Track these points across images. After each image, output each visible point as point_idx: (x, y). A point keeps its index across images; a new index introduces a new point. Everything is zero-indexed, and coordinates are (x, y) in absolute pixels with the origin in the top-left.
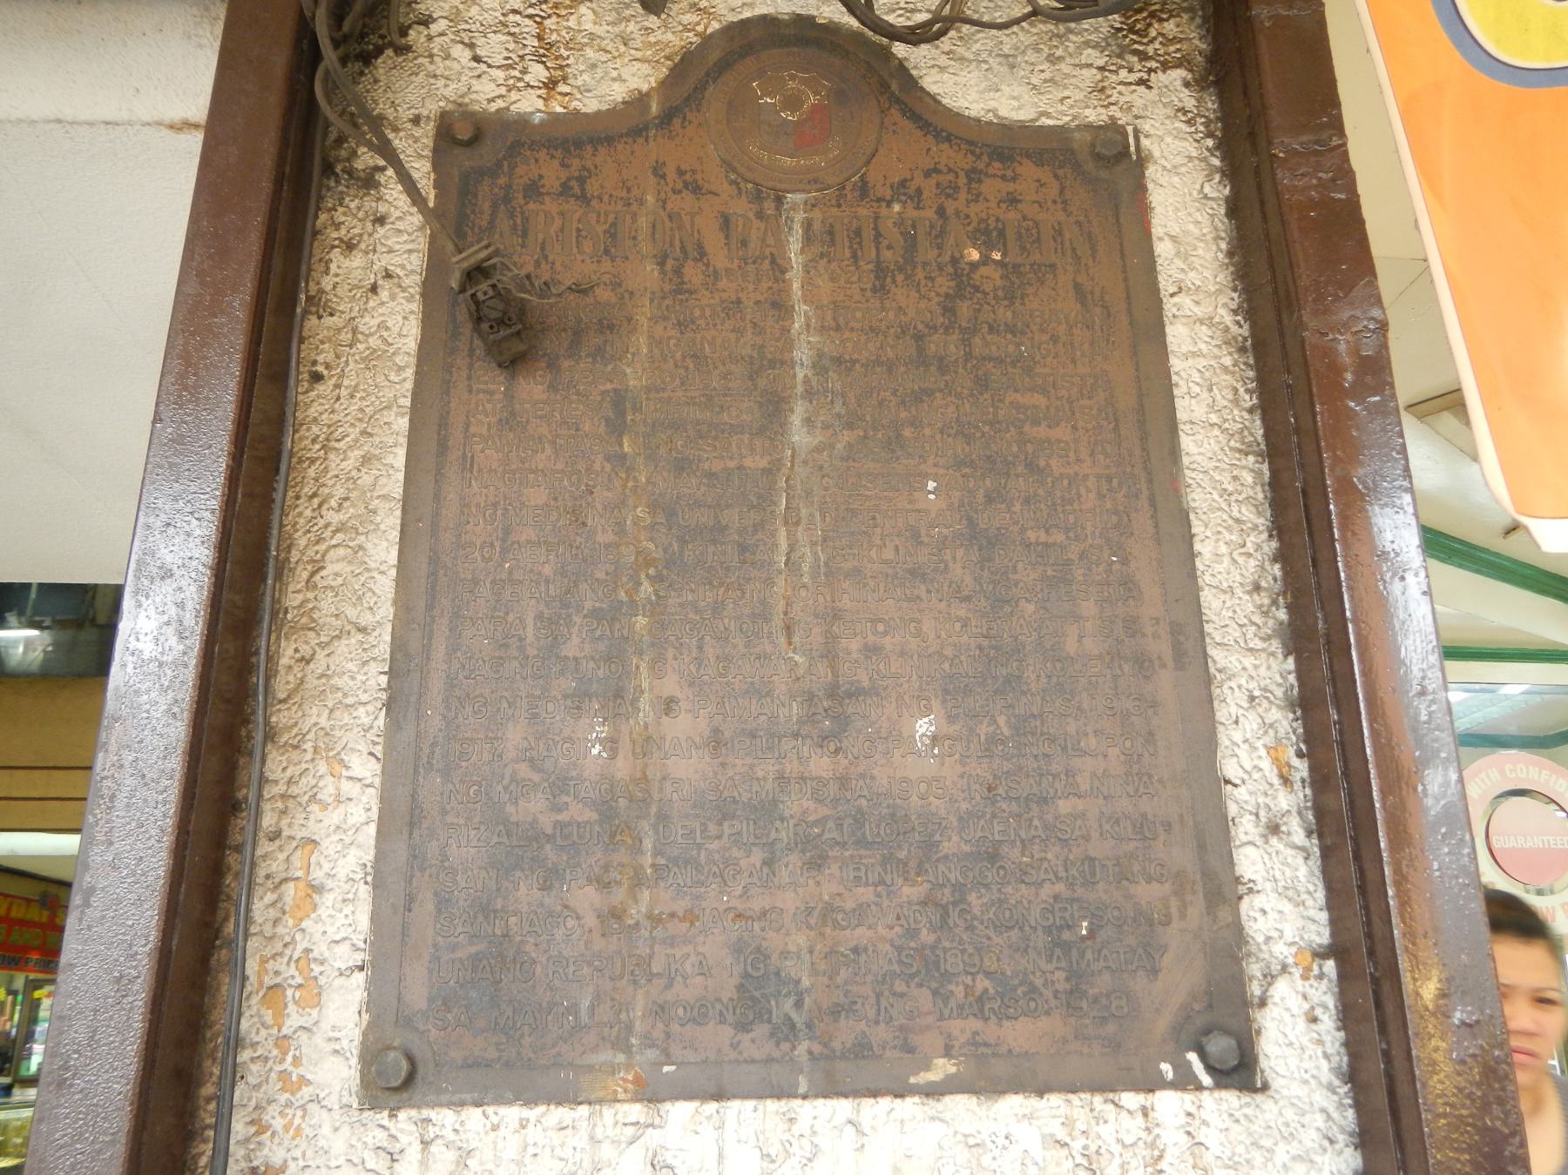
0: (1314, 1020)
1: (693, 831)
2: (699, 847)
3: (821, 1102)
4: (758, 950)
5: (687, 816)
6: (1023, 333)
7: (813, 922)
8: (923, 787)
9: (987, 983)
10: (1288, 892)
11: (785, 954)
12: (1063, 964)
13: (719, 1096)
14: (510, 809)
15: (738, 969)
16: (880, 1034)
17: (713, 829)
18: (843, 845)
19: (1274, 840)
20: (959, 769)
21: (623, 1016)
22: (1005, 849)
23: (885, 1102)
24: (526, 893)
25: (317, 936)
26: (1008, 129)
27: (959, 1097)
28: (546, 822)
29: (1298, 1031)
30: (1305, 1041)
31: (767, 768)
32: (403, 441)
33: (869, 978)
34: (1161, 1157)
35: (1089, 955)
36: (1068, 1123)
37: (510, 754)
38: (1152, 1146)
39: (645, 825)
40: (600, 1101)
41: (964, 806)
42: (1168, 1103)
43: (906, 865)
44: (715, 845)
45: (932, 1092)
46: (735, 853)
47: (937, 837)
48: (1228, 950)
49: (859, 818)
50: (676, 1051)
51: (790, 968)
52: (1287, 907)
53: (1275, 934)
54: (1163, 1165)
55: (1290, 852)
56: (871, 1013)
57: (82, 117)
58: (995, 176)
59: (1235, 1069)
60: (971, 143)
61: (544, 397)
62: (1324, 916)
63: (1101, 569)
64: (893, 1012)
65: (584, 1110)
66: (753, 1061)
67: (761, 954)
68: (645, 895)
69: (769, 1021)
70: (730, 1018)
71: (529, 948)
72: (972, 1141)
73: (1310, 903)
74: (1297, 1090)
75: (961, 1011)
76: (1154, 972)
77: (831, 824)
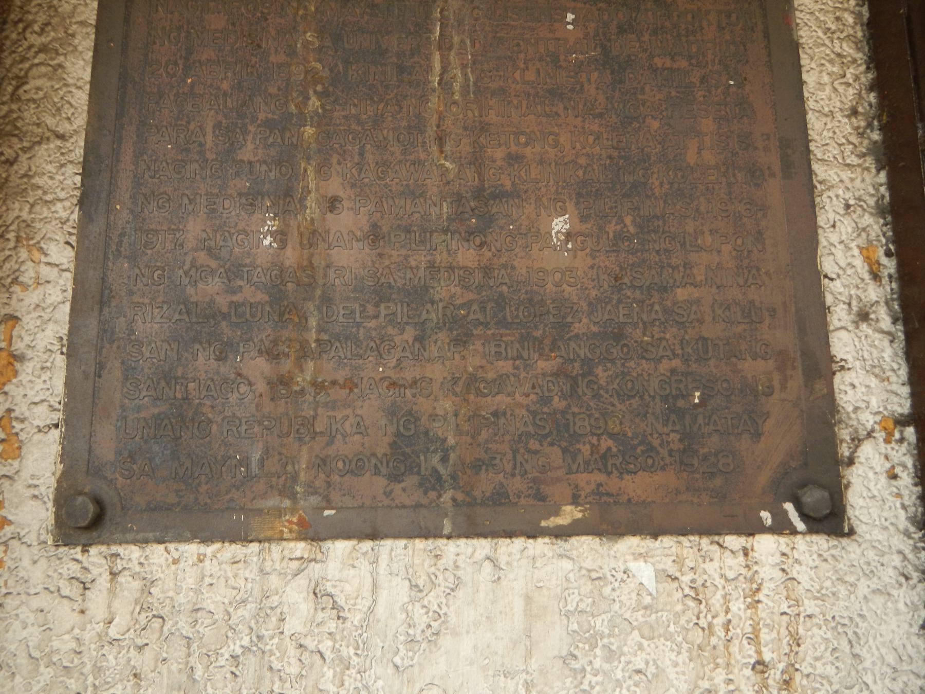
0: (895, 477)
1: (353, 312)
2: (359, 325)
3: (462, 542)
4: (410, 413)
5: (348, 299)
7: (458, 389)
8: (558, 276)
9: (610, 443)
10: (876, 371)
11: (433, 417)
13: (374, 535)
14: (190, 290)
15: (391, 429)
16: (517, 484)
17: (371, 310)
18: (486, 325)
19: (864, 326)
20: (589, 261)
21: (289, 468)
22: (629, 330)
23: (519, 543)
24: (204, 362)
25: (18, 399)
27: (584, 538)
28: (222, 302)
30: (886, 494)
31: (419, 259)
33: (507, 438)
34: (758, 590)
35: (700, 420)
36: (679, 561)
37: (190, 244)
38: (751, 580)
39: (311, 306)
40: (269, 540)
41: (594, 293)
43: (541, 342)
44: (372, 324)
45: (561, 533)
46: (390, 330)
47: (569, 319)
48: (823, 415)
49: (501, 302)
50: (336, 497)
51: (438, 428)
52: (873, 382)
53: (863, 405)
54: (760, 596)
55: (877, 335)
56: (509, 468)
59: (826, 517)
62: (906, 390)
63: (719, 91)
64: (528, 467)
65: (254, 547)
66: (404, 507)
67: (412, 417)
68: (310, 365)
69: (419, 473)
70: (384, 470)
71: (205, 410)
72: (594, 575)
73: (894, 379)
74: (877, 535)
75: (587, 467)
76: (757, 435)
77: (475, 307)
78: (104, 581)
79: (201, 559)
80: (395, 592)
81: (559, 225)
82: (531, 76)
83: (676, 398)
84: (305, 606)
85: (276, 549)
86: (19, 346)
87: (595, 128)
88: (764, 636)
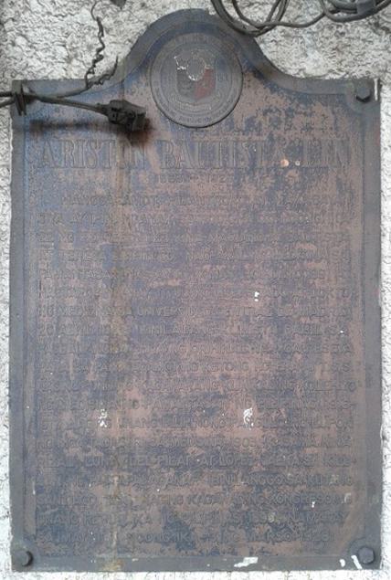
6: (307, 210)
9: (269, 527)
12: (303, 520)
18: (209, 467)
26: (311, 80)
32: (8, 272)
41: (264, 450)
46: (163, 470)
47: (250, 464)
56: (219, 539)
58: (300, 113)
61: (72, 248)
81: (247, 413)
82: (235, 330)
83: (303, 504)
87: (268, 359)
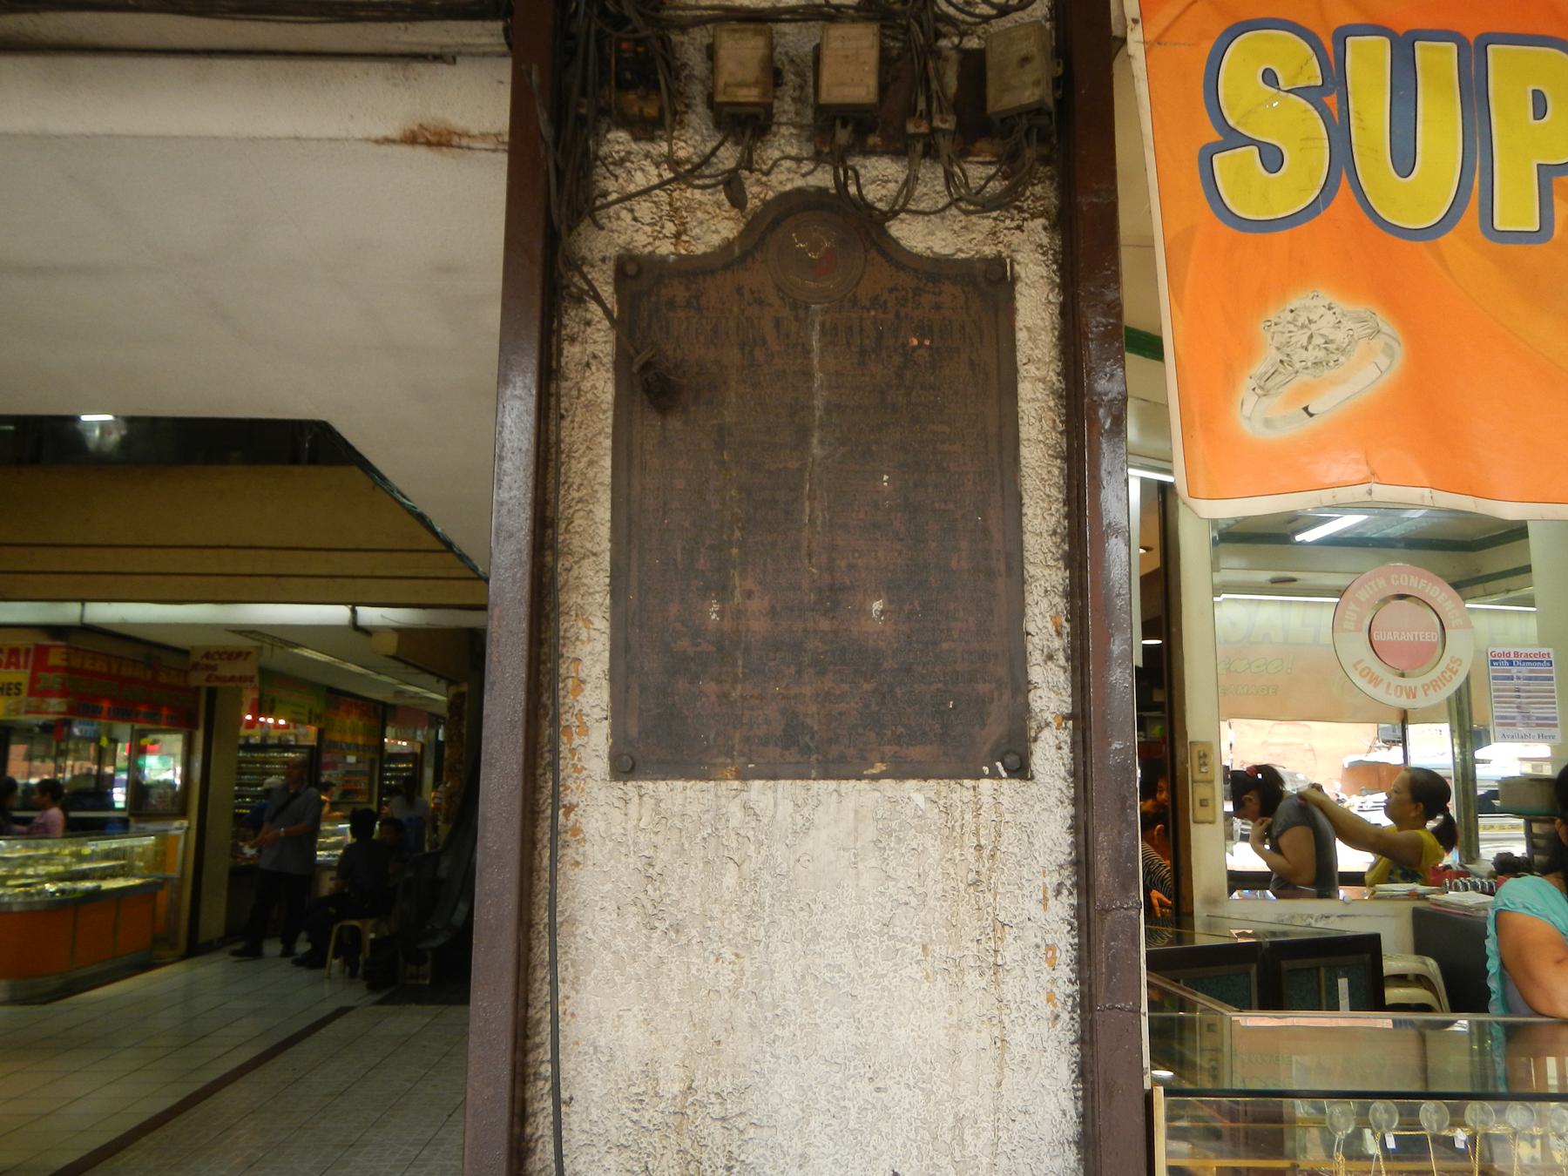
11: (806, 715)
13: (775, 777)
17: (771, 655)
23: (852, 782)
24: (682, 685)
28: (691, 652)
29: (1051, 754)
36: (938, 793)
39: (738, 654)
42: (986, 785)
44: (772, 664)
45: (875, 778)
48: (1022, 713)
51: (809, 721)
57: (315, 134)
60: (916, 271)
68: (739, 687)
74: (1048, 779)
75: (889, 743)
76: (983, 725)
78: (636, 799)
79: (685, 789)
80: (786, 808)
84: (740, 814)
85: (723, 784)
86: (582, 675)
88: (982, 832)
